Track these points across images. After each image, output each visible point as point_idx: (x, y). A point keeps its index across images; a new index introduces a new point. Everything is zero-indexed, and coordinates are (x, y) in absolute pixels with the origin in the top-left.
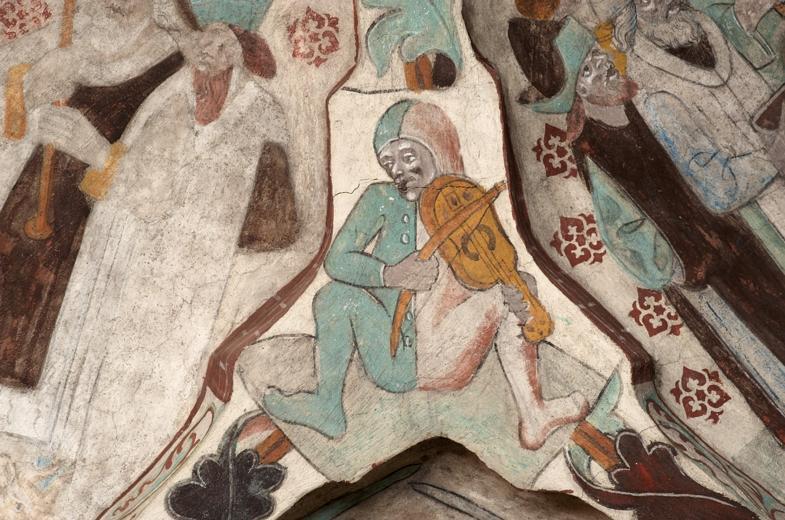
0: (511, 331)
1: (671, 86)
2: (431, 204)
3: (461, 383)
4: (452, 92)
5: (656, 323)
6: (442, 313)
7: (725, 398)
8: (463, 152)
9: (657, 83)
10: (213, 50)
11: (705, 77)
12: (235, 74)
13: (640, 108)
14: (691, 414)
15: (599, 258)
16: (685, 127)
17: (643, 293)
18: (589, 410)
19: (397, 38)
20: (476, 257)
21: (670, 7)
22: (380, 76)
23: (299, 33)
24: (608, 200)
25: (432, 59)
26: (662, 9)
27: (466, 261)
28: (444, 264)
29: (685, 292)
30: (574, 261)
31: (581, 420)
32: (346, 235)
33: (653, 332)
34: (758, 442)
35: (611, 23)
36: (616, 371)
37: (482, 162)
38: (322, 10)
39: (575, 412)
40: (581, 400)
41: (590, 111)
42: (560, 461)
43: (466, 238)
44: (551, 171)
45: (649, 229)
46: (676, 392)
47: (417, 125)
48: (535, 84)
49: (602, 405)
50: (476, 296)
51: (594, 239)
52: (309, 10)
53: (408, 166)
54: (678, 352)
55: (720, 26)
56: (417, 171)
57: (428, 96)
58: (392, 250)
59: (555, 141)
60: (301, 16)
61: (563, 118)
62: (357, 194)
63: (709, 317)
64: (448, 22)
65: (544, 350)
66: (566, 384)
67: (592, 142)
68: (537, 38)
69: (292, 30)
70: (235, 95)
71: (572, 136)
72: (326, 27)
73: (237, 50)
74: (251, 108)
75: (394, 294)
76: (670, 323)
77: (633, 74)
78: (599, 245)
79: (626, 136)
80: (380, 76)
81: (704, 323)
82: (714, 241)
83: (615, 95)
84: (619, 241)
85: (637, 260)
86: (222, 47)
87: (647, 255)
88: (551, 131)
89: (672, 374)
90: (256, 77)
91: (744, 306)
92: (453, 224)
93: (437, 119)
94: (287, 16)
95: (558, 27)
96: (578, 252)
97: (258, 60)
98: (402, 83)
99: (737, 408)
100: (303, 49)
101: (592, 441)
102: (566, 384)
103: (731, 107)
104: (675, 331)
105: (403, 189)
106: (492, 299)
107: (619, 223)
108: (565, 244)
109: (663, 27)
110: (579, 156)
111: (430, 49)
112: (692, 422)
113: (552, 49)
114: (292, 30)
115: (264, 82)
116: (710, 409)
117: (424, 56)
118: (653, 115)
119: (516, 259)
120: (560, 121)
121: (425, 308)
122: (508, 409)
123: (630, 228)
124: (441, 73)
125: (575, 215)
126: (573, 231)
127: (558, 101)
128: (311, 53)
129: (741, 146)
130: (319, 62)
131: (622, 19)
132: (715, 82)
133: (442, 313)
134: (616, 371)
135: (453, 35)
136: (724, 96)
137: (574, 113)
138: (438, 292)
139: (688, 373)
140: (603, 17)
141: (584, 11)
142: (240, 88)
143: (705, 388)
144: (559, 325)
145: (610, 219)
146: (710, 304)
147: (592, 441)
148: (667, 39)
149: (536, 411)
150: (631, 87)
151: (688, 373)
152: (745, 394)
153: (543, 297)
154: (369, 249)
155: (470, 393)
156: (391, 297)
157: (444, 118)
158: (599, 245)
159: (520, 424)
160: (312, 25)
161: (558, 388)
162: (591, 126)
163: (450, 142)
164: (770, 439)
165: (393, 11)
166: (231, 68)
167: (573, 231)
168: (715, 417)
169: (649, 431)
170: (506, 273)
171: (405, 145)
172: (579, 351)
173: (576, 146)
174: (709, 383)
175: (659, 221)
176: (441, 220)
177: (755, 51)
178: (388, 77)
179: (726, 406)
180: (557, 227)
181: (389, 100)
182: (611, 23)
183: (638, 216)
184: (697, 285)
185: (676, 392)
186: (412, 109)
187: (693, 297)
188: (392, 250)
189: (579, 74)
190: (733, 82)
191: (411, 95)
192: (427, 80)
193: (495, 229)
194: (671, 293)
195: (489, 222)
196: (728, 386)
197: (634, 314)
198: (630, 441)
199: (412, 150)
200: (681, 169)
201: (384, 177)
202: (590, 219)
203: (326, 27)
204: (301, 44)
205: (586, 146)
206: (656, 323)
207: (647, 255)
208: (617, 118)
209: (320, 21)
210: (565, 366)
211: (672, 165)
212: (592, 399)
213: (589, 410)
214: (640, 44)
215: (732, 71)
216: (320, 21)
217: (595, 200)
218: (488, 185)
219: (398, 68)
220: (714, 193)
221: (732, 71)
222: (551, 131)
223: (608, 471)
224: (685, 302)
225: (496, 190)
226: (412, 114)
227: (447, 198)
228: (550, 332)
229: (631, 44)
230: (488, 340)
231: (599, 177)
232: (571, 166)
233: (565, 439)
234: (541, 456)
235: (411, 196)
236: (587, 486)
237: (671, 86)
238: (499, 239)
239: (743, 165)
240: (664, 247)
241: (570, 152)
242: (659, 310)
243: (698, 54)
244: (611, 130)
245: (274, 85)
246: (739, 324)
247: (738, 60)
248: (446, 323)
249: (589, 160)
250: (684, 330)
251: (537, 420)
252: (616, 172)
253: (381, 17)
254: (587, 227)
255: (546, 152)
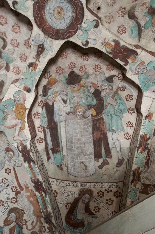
0: (18, 127)
1: (60, 103)
2: (18, 105)
3: (10, 128)
4: (28, 93)
5: (40, 130)
6: (11, 119)
7: (43, 142)
8: (26, 101)
9: (58, 102)
10: (2, 63)
11: (64, 105)
12: (3, 68)
13: (54, 104)
14: (37, 143)
15: (38, 119)
16: (58, 109)
17: (41, 126)
18: (23, 141)
19: (25, 82)
20: (20, 115)
21: (65, 94)
22: (20, 86)
23: (15, 69)
24: (43, 113)
25: (28, 88)
26: (64, 94)
27: (18, 115)
28: (15, 114)
29: (46, 128)
30: (35, 118)
31: (22, 141)
32: (3, 103)
33: (39, 131)
34: (43, 149)
35: (57, 92)
36: (29, 139)
37: (27, 104)
38: (20, 68)
39: (21, 140)
40: (23, 139)
41: (48, 101)
42: (17, 144)
43: (20, 112)
44: (39, 105)
45: (46, 119)
46: (37, 139)
47: (21, 95)
48: (43, 94)
49: (25, 141)
50: (17, 120)
51: (39, 116)
52: (18, 67)
53: (17, 99)
54: (40, 135)
55: (70, 100)
56: (18, 100)
57: (25, 92)
58: (9, 108)
59: (41, 102)
60: (17, 67)
61: (44, 100)
62: (8, 99)
63: (47, 132)
64: (33, 84)
65: (22, 131)
66: (22, 136)
67: (46, 105)
68: (47, 89)
69: (14, 68)
70: (1, 71)
71: (44, 103)
72: (19, 71)
73: (5, 65)
74: (3, 74)
75: (6, 113)
76: (42, 131)
77: (56, 100)
78: (39, 117)
79: (51, 106)
80: (20, 86)
81: (46, 133)
82: (53, 124)
83: (52, 101)
84: (42, 118)
85: (43, 121)
86: (3, 63)
87: (44, 122)
88: (42, 101)
89: (38, 137)
90: (6, 71)
91: (51, 133)
92: (19, 109)
93: (25, 96)
94: (15, 65)
95: (50, 89)
96: (36, 117)
97: (7, 68)
98: (22, 88)
99: (43, 145)
100: (14, 71)
101: (22, 144)
102: (22, 136)
103: (65, 110)
104: (42, 132)
105: (15, 102)
106: (19, 121)
107: (43, 116)
108: (35, 115)
109: (63, 96)
110: (43, 105)
111: (29, 86)
112: (37, 144)
113: (48, 91)
114: (14, 68)
115: (7, 72)
116: (40, 143)
117: (27, 87)
118: (56, 106)
119: (25, 118)
120: (43, 100)
121: (9, 117)
122: (14, 134)
123: (44, 117)
124: (29, 91)
125: (38, 112)
126: (37, 114)
127: (45, 98)
128: (15, 73)
129: (63, 115)
130: (15, 74)
131: (59, 92)
132: (65, 106)
133: (11, 119)
134: (29, 139)
135: (33, 87)
136: (65, 108)
137: (46, 100)
138: (12, 116)
139: (40, 138)
140: (57, 91)
141: (55, 89)
142: (3, 70)
143: (41, 140)
144: (25, 129)
145: (42, 115)
146: (48, 131)
147: (22, 144)
148: (63, 98)
149: (17, 137)
150: (55, 101)
151: (40, 138)
152: (45, 143)
153: (25, 125)
154: (6, 106)
155: (10, 130)
156: (5, 114)
157: (26, 96)
158: (39, 117)
159: (14, 137)
160: (17, 69)
161: (21, 136)
162: (47, 102)
163: (25, 100)
164: (45, 149)
165: (26, 78)
166: (3, 67)
167: (37, 114)
168: (40, 144)
169: (29, 147)
170: (22, 119)
171: (18, 96)
172: (26, 134)
173: (44, 104)
174: (42, 140)
175: (48, 118)
176: (18, 108)
177: (72, 105)
178: (21, 86)
179: (42, 144)
180: (35, 113)
181: (19, 89)
182: (57, 92)
183: (46, 116)
184: (47, 128)
185: (37, 139)
186: (22, 92)
187: (46, 129)
188: (9, 108)
189: (49, 96)
190: (67, 107)
191: (23, 91)
192: (26, 90)
193: (24, 113)
194: (44, 127)
195: (24, 112)
196: (44, 141)
197: (38, 128)
198: (26, 147)
199: (19, 98)
200: (54, 113)
201: (13, 99)
202: (40, 114)
203: (19, 71)
204: (14, 70)
205: (45, 105)
206: (40, 130)
207: (44, 122)
208: (51, 104)
209: (19, 69)
210: (23, 134)
211: (54, 113)
212: (24, 140)
213: (23, 141)
214: (59, 96)
215: (67, 106)
216: (19, 69)
217: (42, 112)
218: (27, 107)
219: (23, 86)
220: (56, 119)
221: (67, 106)
222: (42, 101)
223: (21, 148)
224: (45, 129)
225: (27, 109)
226: (21, 93)
227: (20, 106)
228: (24, 129)
229: (58, 96)
230: (16, 125)
231: (44, 109)
232: (42, 106)
233: (19, 142)
234: (14, 142)
235: (15, 103)
236: (18, 148)
237: (60, 103)
238: (24, 115)
239: (62, 117)
240: (47, 122)
241: (42, 104)
242: (41, 129)
243: (65, 102)
244: (49, 104)
245: (8, 73)
246: (49, 135)
247: (69, 105)
248: (11, 121)
249: (44, 107)
250: (43, 133)
251: (16, 138)
252: (47, 110)
253: (24, 78)
254: (39, 114)
255: (39, 103)
